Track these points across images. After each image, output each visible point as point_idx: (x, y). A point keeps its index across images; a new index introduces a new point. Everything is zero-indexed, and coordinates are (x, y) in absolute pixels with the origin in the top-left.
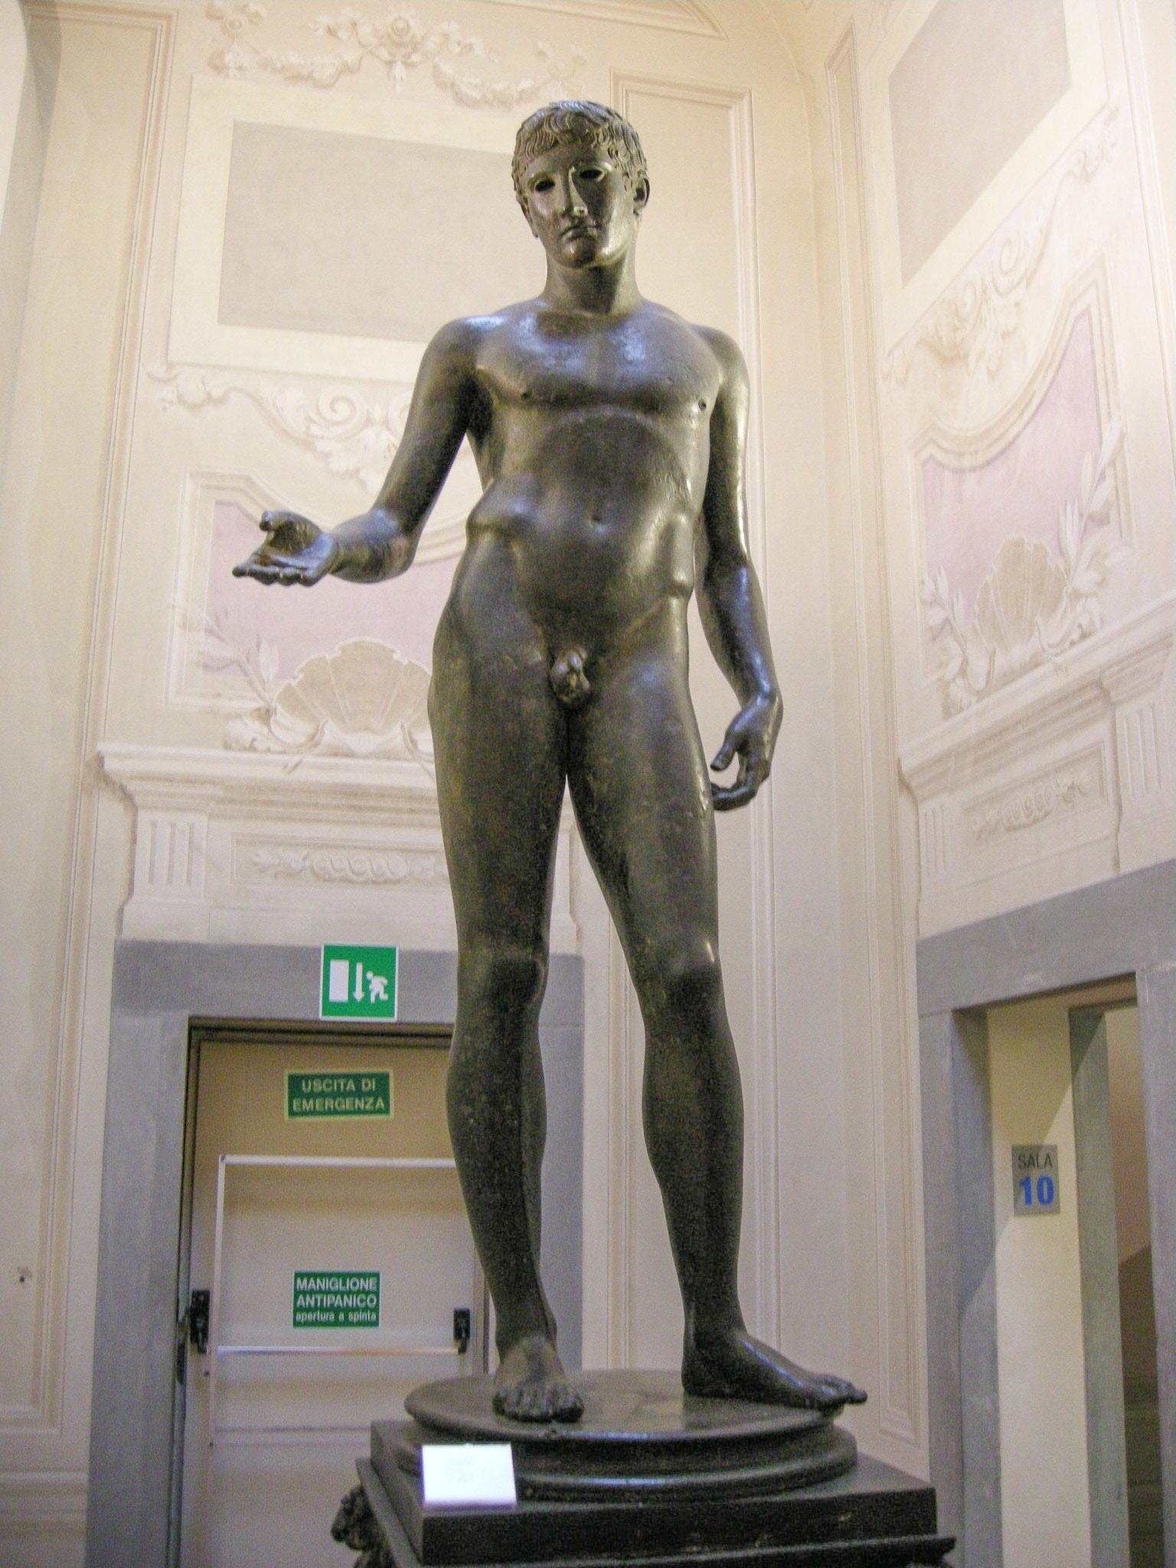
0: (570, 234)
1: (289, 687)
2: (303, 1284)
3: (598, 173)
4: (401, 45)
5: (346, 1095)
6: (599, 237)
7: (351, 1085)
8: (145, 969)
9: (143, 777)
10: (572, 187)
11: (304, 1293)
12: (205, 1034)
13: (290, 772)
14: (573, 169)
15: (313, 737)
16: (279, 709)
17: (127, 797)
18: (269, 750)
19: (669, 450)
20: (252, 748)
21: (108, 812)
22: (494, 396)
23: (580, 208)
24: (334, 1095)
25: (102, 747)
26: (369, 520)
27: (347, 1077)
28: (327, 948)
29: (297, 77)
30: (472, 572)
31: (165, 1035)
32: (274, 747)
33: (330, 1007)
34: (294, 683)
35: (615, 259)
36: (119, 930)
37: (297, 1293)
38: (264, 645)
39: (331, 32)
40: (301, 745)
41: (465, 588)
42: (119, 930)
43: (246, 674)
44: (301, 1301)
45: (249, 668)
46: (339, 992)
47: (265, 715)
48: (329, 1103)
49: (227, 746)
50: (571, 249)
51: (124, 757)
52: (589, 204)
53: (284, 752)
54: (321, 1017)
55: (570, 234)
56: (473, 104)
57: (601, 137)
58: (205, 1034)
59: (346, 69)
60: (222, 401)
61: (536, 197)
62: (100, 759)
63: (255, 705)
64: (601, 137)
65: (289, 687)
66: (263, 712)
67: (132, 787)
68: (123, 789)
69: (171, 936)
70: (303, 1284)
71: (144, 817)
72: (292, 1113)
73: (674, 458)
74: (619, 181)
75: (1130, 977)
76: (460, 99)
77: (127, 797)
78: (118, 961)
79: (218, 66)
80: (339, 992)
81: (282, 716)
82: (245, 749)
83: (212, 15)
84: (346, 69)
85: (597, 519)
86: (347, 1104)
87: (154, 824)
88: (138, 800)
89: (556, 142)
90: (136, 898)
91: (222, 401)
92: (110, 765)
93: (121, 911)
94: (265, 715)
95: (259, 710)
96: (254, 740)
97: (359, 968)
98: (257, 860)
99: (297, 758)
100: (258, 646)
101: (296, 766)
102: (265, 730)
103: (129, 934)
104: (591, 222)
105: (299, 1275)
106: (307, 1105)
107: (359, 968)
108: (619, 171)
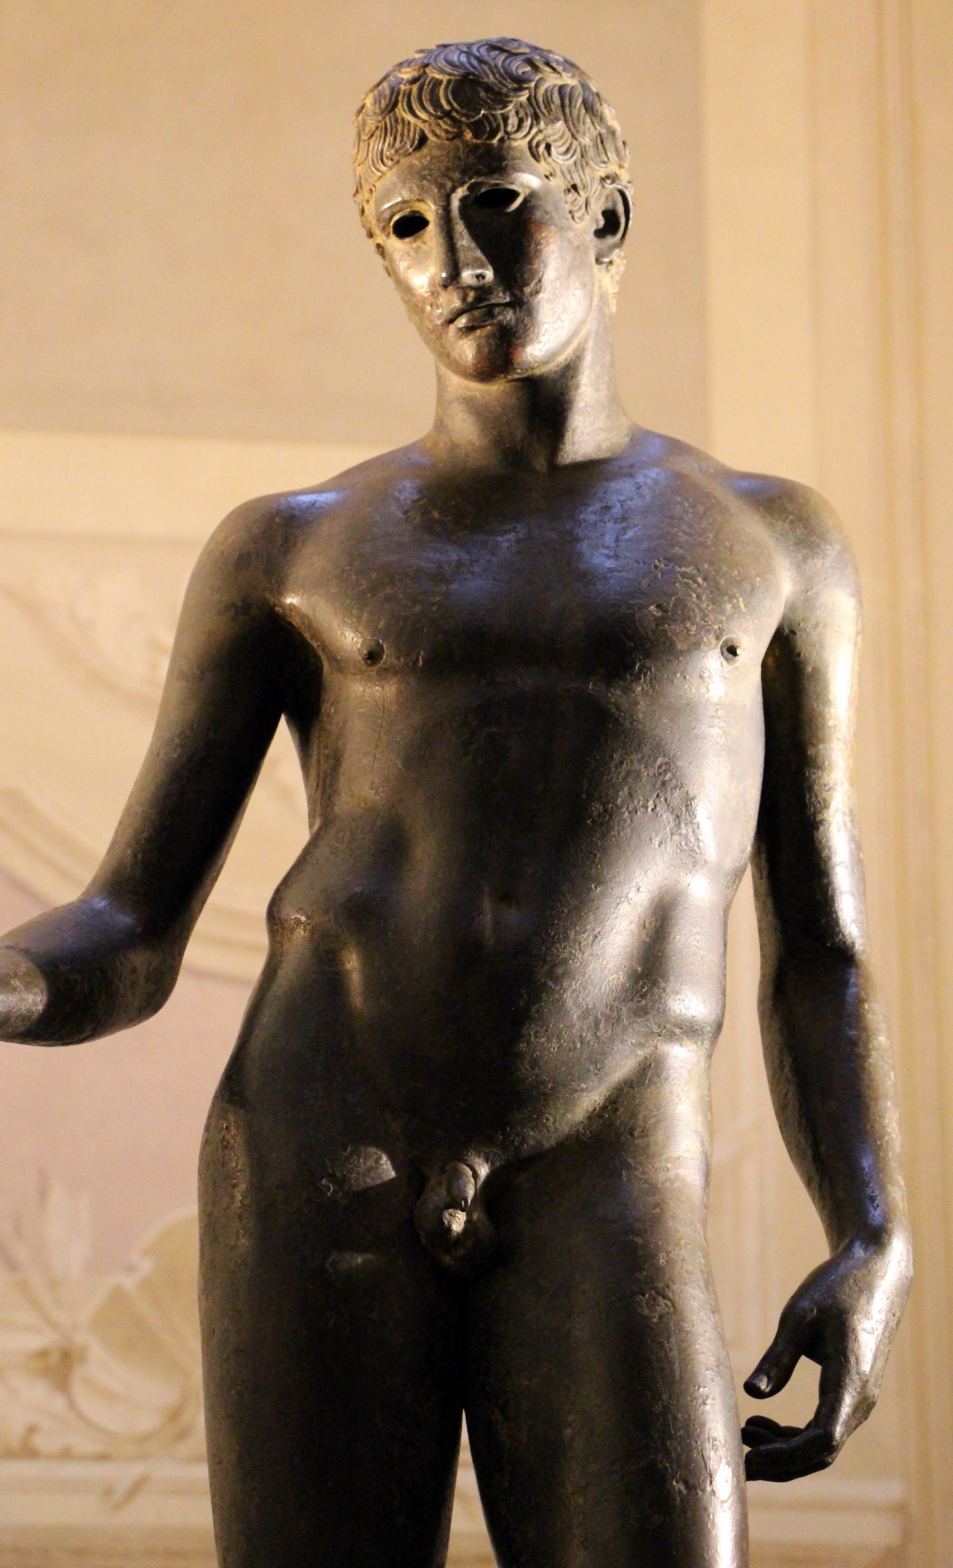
0: (462, 321)
1: (118, 1296)
3: (514, 195)
6: (519, 321)
10: (460, 227)
13: (118, 1506)
14: (461, 192)
15: (174, 1414)
16: (96, 1350)
18: (66, 1455)
19: (659, 748)
20: (28, 1452)
22: (323, 658)
23: (478, 272)
26: (79, 914)
30: (267, 1017)
32: (85, 1445)
34: (129, 1282)
35: (561, 359)
38: (57, 1195)
40: (147, 1438)
41: (256, 1045)
43: (13, 1266)
45: (20, 1252)
47: (59, 1366)
50: (467, 350)
52: (494, 260)
53: (103, 1457)
55: (462, 321)
57: (513, 121)
61: (395, 244)
64: (513, 121)
65: (118, 1296)
66: (55, 1358)
73: (668, 766)
74: (558, 203)
81: (102, 1366)
85: (505, 897)
89: (423, 139)
94: (59, 1366)
95: (43, 1354)
96: (32, 1429)
99: (136, 1470)
100: (43, 1194)
101: (134, 1490)
102: (59, 1403)
104: (502, 297)
108: (558, 183)
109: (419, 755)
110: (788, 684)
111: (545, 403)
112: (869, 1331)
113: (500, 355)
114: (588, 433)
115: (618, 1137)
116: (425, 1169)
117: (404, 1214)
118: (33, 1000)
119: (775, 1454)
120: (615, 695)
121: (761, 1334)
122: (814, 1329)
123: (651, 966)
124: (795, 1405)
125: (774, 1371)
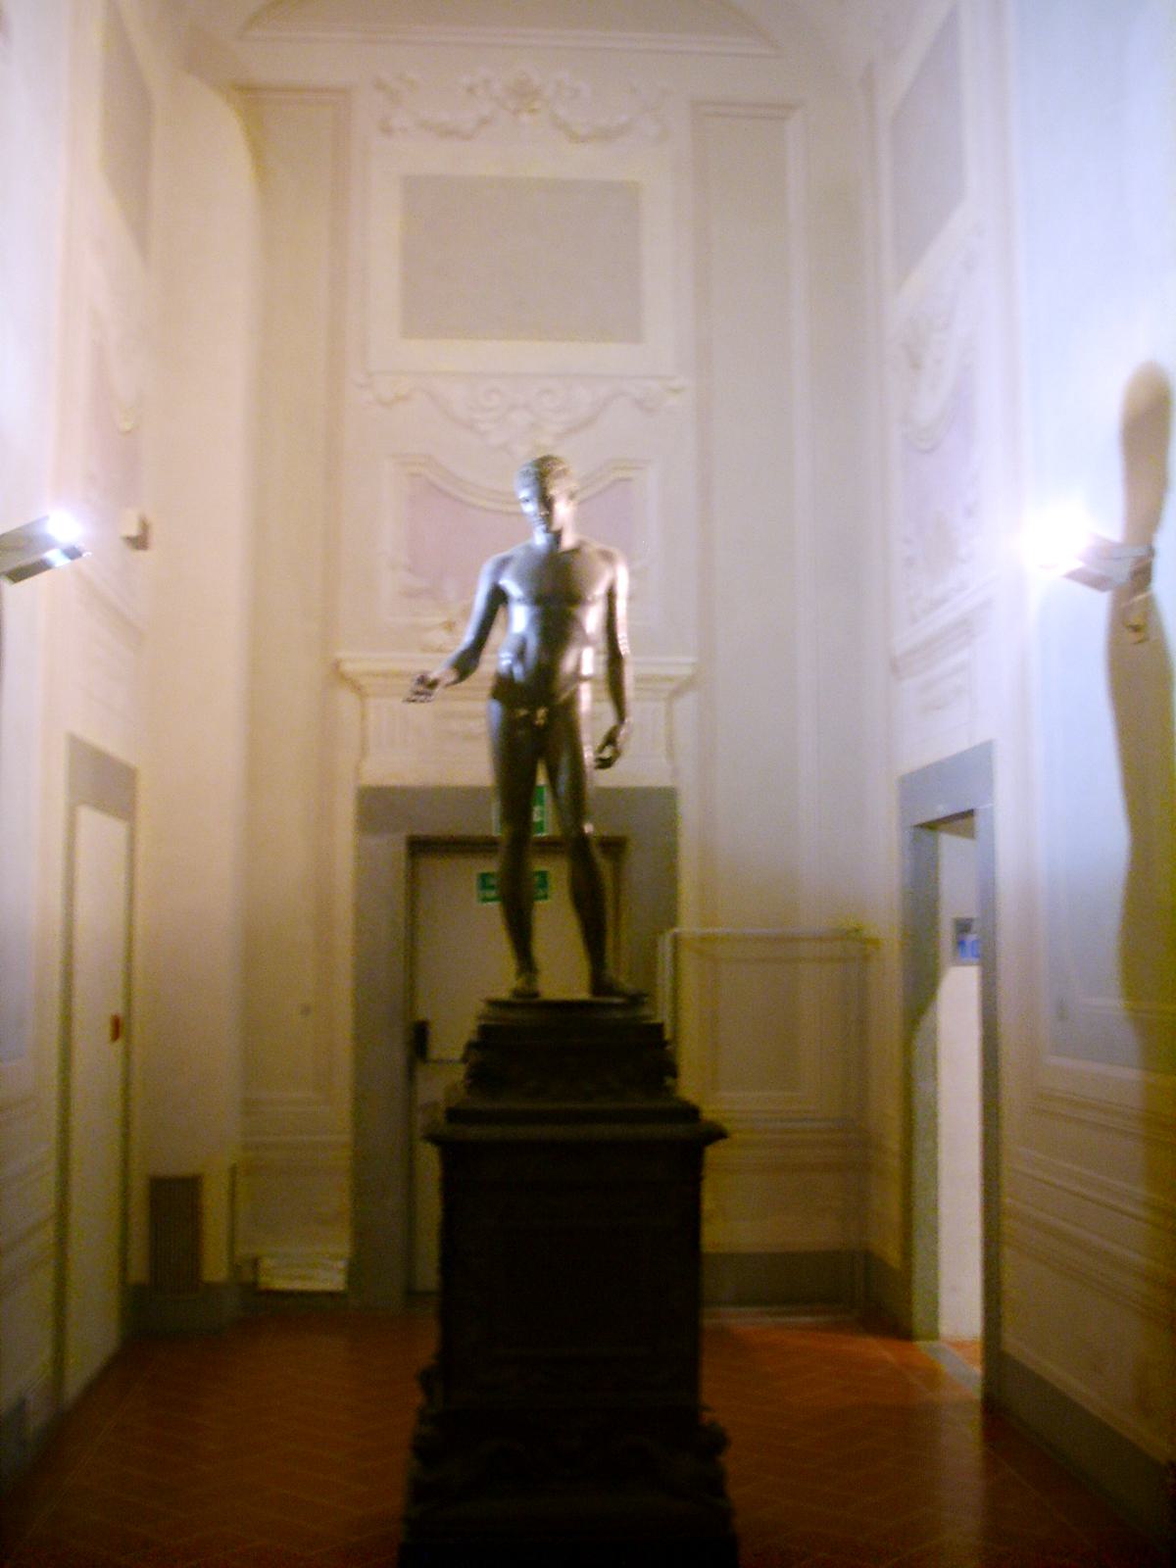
4: (524, 94)
8: (378, 806)
12: (420, 847)
17: (357, 688)
21: (346, 700)
25: (341, 654)
29: (449, 133)
31: (392, 848)
39: (471, 90)
51: (355, 661)
56: (583, 140)
58: (420, 847)
59: (484, 122)
60: (405, 398)
62: (337, 665)
63: (439, 619)
69: (392, 782)
75: (969, 814)
76: (575, 138)
77: (357, 688)
79: (387, 130)
83: (380, 86)
84: (484, 122)
91: (405, 398)
92: (347, 667)
95: (445, 622)
109: (533, 620)
110: (611, 596)
111: (557, 537)
112: (620, 739)
113: (547, 530)
114: (568, 541)
115: (572, 703)
116: (533, 711)
117: (529, 720)
118: (453, 677)
119: (605, 764)
120: (572, 609)
121: (599, 740)
122: (611, 739)
123: (578, 667)
124: (607, 753)
125: (601, 749)
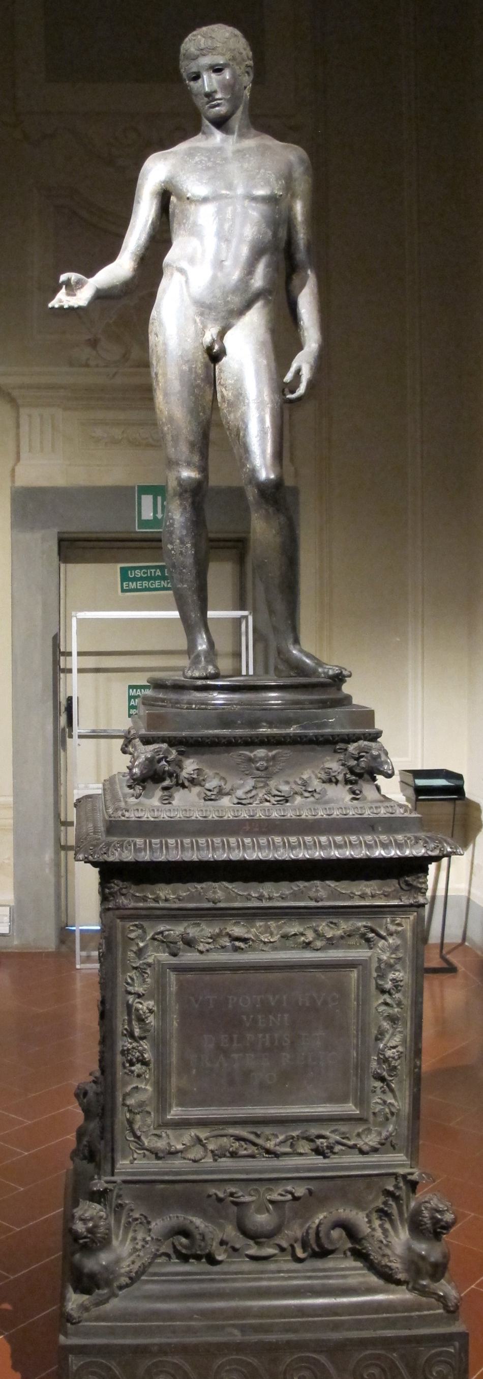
2: (133, 692)
5: (155, 578)
7: (159, 573)
9: (21, 387)
11: (135, 697)
18: (97, 366)
20: (87, 365)
24: (148, 579)
27: (156, 567)
28: (139, 486)
33: (144, 523)
36: (13, 481)
37: (130, 698)
42: (13, 481)
44: (132, 703)
46: (147, 514)
47: (93, 343)
48: (145, 584)
49: (71, 365)
53: (106, 366)
54: (137, 530)
63: (87, 337)
67: (15, 393)
68: (9, 394)
70: (133, 692)
71: (22, 410)
72: (123, 591)
78: (14, 500)
80: (147, 514)
82: (81, 366)
86: (157, 584)
87: (30, 416)
88: (20, 402)
90: (21, 462)
93: (13, 470)
95: (89, 340)
96: (88, 359)
97: (159, 498)
98: (93, 434)
99: (115, 370)
102: (94, 353)
103: (19, 483)
105: (131, 687)
106: (133, 585)
107: (159, 498)
